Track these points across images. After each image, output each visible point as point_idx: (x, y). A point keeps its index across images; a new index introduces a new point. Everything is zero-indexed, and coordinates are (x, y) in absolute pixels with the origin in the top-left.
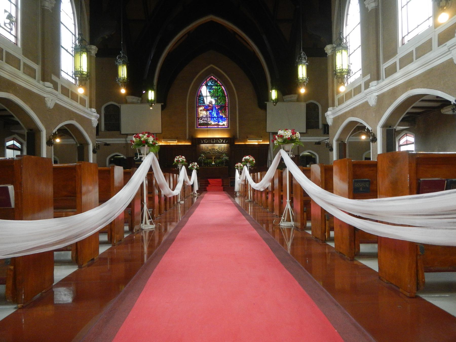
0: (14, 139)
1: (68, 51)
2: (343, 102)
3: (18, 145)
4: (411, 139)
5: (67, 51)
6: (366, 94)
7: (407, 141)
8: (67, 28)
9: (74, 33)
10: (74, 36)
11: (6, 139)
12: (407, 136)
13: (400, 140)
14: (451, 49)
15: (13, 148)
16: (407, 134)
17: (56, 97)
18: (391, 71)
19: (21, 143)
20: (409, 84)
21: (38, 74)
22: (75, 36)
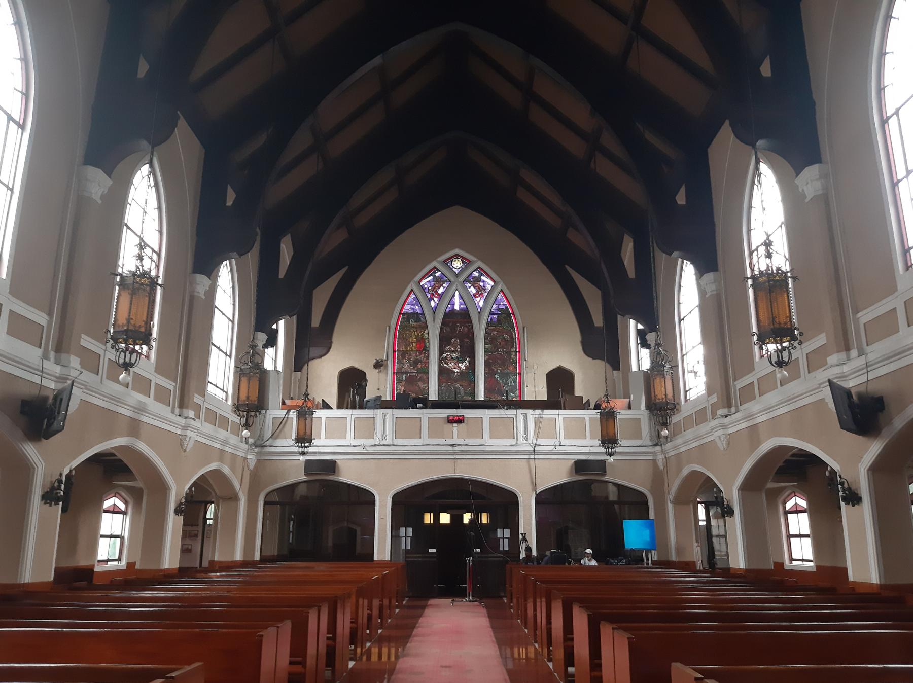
0: (117, 495)
1: (221, 348)
2: (681, 433)
3: (122, 506)
4: (803, 503)
5: (219, 349)
6: (712, 429)
7: (796, 504)
8: (223, 314)
9: (231, 319)
10: (230, 323)
11: (104, 496)
12: (795, 496)
13: (785, 503)
14: (822, 386)
15: (114, 510)
16: (795, 494)
17: (196, 431)
18: (748, 394)
19: (126, 503)
20: (775, 426)
21: (175, 398)
22: (233, 322)
